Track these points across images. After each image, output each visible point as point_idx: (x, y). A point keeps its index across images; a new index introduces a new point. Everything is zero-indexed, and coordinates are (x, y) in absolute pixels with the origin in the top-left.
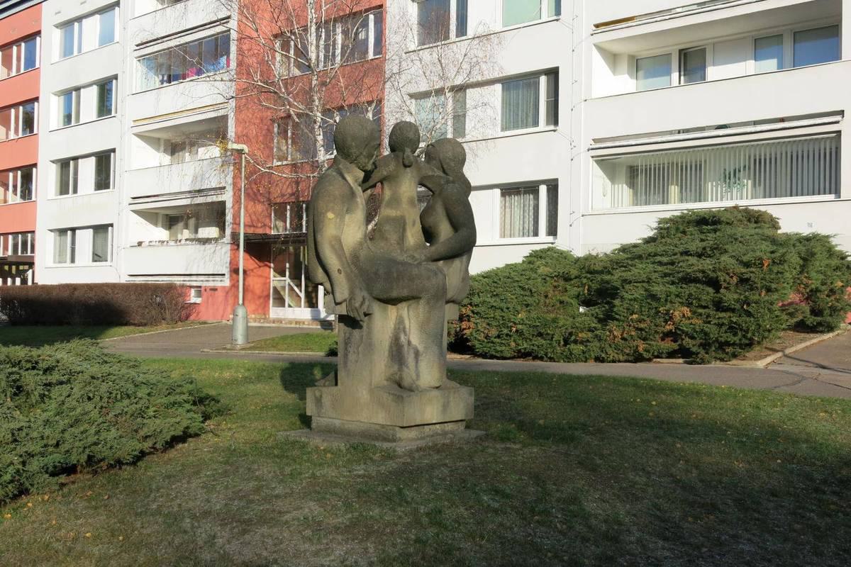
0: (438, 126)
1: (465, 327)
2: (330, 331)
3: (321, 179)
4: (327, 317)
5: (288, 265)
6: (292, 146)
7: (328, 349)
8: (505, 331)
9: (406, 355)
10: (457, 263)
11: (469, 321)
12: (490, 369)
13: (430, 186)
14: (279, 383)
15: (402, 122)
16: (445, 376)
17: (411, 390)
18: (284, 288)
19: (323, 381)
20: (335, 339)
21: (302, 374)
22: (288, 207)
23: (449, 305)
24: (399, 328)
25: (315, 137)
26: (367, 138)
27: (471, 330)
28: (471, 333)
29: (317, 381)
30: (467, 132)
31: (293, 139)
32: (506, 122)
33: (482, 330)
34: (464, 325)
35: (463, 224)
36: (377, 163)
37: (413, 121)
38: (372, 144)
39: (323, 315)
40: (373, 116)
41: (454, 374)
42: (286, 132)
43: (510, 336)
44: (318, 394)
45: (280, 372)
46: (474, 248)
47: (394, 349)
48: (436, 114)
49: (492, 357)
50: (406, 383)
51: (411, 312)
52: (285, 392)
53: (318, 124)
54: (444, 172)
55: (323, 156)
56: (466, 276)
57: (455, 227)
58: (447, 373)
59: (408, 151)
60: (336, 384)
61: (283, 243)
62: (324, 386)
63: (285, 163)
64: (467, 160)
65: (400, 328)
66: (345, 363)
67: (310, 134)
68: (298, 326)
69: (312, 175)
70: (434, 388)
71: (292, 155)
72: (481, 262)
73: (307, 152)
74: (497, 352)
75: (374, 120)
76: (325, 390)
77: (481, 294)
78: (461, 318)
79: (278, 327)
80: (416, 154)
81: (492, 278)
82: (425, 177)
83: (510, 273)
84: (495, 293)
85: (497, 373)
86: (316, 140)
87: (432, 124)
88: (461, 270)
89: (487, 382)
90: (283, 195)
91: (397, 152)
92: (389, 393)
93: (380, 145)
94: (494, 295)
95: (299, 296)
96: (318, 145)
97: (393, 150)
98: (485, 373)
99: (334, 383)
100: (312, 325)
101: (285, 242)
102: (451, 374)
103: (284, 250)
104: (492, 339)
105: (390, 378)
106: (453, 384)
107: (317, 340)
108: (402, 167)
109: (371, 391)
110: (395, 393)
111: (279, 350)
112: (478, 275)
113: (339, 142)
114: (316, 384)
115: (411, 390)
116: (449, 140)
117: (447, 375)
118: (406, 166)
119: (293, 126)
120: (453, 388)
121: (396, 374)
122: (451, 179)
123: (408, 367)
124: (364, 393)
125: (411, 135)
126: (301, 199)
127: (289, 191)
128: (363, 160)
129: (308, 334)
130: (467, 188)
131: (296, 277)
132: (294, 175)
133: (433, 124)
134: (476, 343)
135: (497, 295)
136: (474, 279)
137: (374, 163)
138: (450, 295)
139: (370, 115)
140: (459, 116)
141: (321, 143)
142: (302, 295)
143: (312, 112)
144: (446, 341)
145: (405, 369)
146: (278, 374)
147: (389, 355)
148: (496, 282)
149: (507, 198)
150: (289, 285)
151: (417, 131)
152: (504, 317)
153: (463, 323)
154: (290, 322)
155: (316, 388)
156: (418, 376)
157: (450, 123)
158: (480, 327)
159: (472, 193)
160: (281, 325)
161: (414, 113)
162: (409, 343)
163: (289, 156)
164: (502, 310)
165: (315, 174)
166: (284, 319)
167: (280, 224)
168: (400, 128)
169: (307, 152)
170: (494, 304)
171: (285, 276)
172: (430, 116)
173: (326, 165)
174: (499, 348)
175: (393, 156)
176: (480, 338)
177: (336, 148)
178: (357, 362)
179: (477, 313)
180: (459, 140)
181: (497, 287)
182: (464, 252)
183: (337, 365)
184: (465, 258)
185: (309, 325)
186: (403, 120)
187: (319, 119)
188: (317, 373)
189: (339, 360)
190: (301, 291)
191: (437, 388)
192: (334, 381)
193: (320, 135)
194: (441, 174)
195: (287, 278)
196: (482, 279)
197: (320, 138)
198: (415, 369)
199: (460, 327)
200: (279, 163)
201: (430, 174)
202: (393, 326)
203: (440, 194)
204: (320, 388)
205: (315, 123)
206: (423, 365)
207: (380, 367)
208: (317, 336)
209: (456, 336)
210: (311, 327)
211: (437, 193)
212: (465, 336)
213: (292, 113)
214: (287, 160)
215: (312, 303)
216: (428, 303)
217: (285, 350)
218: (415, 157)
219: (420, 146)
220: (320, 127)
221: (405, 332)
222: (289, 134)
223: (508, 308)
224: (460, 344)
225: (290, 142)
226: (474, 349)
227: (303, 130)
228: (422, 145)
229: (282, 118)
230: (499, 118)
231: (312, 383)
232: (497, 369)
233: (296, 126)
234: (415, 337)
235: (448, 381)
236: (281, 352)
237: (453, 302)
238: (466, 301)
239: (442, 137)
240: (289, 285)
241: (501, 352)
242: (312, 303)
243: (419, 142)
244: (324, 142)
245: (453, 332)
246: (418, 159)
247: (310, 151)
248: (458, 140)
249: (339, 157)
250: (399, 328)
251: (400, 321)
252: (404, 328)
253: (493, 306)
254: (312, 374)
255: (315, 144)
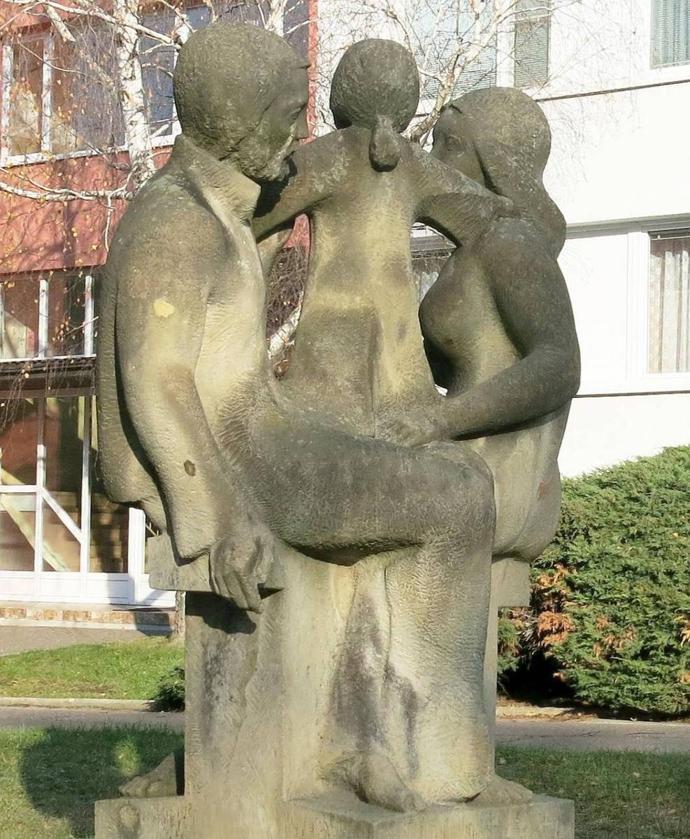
0: (471, 54)
1: (548, 627)
2: (160, 639)
3: (138, 202)
4: (153, 598)
5: (41, 450)
6: (55, 110)
7: (157, 691)
8: (664, 639)
9: (379, 709)
10: (525, 443)
11: (559, 609)
12: (619, 747)
13: (447, 225)
14: (18, 786)
15: (368, 41)
16: (490, 767)
17: (393, 807)
18: (30, 515)
19: (142, 782)
20: (177, 663)
21: (84, 761)
22: (44, 285)
23: (502, 564)
24: (359, 630)
25: (119, 85)
26: (267, 87)
27: (565, 634)
28: (565, 644)
29: (124, 780)
30: (553, 69)
31: (56, 90)
32: (665, 42)
33: (598, 636)
34: (546, 620)
35: (542, 331)
36: (297, 161)
37: (399, 39)
38: (284, 104)
39: (142, 592)
40: (287, 24)
41: (516, 762)
42: (37, 69)
43: (678, 653)
44: (127, 818)
45: (20, 754)
46: (575, 402)
47: (346, 688)
48: (466, 21)
49: (626, 713)
50: (381, 784)
51: (394, 584)
52: (35, 814)
53: (130, 47)
54: (489, 183)
55: (145, 139)
56: (551, 484)
57: (520, 340)
58: (497, 760)
59: (385, 124)
60: (180, 791)
61: (30, 386)
62: (146, 794)
63: (34, 158)
64: (554, 150)
65: (362, 627)
66: (207, 732)
67: (105, 77)
68: (69, 624)
69: (110, 194)
70: (459, 802)
71: (53, 137)
72: (603, 436)
73: (98, 127)
74: (640, 698)
75: (289, 37)
76: (147, 806)
77: (592, 533)
78: (537, 603)
79: (14, 628)
80: (408, 133)
81: (624, 487)
82: (434, 199)
83: (676, 474)
84: (633, 530)
85: (637, 758)
86: (122, 93)
87: (455, 46)
88: (535, 467)
89: (610, 785)
90: (28, 251)
91: (353, 127)
92: (332, 817)
93: (304, 106)
94: (632, 537)
95: (71, 538)
96: (128, 106)
97: (342, 120)
98: (605, 758)
99: (174, 788)
100: (111, 621)
101: (35, 385)
102: (509, 762)
103: (34, 408)
104: (626, 661)
105: (334, 774)
106: (516, 790)
107: (124, 663)
108: (368, 171)
109: (281, 811)
110: (348, 815)
111: (16, 693)
112: (586, 480)
113: (192, 105)
114: (123, 789)
115: (393, 807)
116: (502, 94)
117: (497, 763)
118: (378, 168)
119: (56, 52)
120: (513, 801)
121: (352, 761)
122: (508, 203)
123: (383, 742)
124: (261, 813)
125: (394, 78)
126: (80, 262)
127: (47, 238)
128: (255, 150)
129: (99, 647)
130: (554, 229)
131: (65, 484)
132: (59, 194)
133: (457, 47)
134: (581, 674)
135: (639, 534)
136: (574, 490)
137: (288, 160)
138: (505, 534)
139: (276, 22)
140: (531, 24)
141: (138, 100)
142: (84, 535)
143: (110, 13)
144: (493, 666)
145: (376, 745)
146: (14, 762)
147: (331, 709)
148: (636, 500)
149: (669, 257)
150: (46, 506)
151: (411, 66)
152: (659, 598)
153: (544, 615)
154: (50, 614)
155: (122, 800)
156: (414, 766)
157: (505, 43)
158: (590, 629)
159: (570, 244)
160: (23, 622)
161: (401, 15)
162: (389, 673)
163: (46, 139)
164: (654, 578)
165: (121, 191)
166: (32, 604)
167: (19, 332)
168: (360, 59)
169: (98, 127)
170: (631, 562)
171: (34, 483)
172: (450, 25)
173: (151, 164)
174: (644, 688)
175: (341, 138)
176: (590, 659)
177: (180, 117)
178: (239, 726)
179: (583, 588)
180: (533, 93)
181: (638, 514)
182: (545, 414)
183: (183, 736)
184: (547, 429)
185: (101, 620)
186: (372, 35)
187: (133, 35)
188: (126, 758)
189: (187, 721)
190: (79, 525)
191: (469, 800)
192: (174, 781)
193: (133, 77)
194: (481, 190)
195: (40, 488)
196: (595, 488)
197: (134, 88)
198: (404, 746)
199: (535, 626)
200: (18, 160)
201: (449, 189)
202: (341, 625)
203: (476, 249)
204: (133, 801)
205: (120, 43)
206: (429, 734)
207: (305, 741)
208: (127, 653)
209: (522, 652)
210: (107, 626)
211: (467, 244)
212: (548, 654)
213: (54, 15)
214: (38, 149)
215: (111, 558)
216: (443, 559)
217: (36, 692)
218: (406, 140)
219: (420, 110)
220: (133, 55)
221: (376, 642)
222: (47, 76)
223: (670, 574)
224: (533, 678)
225: (47, 97)
226: (573, 691)
227: (84, 65)
228: (426, 106)
229: (25, 30)
230: (646, 29)
231: (112, 788)
232: (640, 749)
233: (65, 52)
234: (404, 656)
235: (498, 779)
236: (22, 700)
237: (515, 555)
238: (551, 554)
239: (482, 86)
240: (46, 506)
241: (652, 697)
242: (111, 558)
243: (416, 98)
244: (145, 97)
245: (513, 642)
246: (414, 146)
247: (104, 126)
248: (529, 92)
249: (188, 141)
250: (359, 630)
251: (363, 610)
252: (375, 630)
253: (626, 568)
254: (111, 761)
255: (119, 105)
